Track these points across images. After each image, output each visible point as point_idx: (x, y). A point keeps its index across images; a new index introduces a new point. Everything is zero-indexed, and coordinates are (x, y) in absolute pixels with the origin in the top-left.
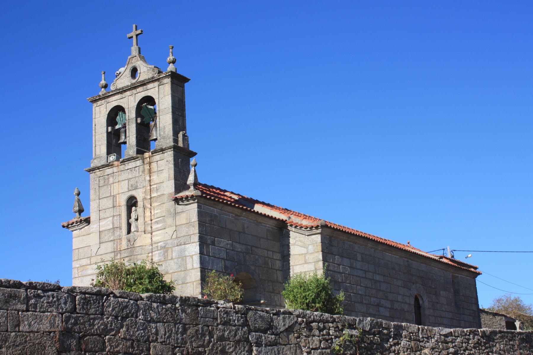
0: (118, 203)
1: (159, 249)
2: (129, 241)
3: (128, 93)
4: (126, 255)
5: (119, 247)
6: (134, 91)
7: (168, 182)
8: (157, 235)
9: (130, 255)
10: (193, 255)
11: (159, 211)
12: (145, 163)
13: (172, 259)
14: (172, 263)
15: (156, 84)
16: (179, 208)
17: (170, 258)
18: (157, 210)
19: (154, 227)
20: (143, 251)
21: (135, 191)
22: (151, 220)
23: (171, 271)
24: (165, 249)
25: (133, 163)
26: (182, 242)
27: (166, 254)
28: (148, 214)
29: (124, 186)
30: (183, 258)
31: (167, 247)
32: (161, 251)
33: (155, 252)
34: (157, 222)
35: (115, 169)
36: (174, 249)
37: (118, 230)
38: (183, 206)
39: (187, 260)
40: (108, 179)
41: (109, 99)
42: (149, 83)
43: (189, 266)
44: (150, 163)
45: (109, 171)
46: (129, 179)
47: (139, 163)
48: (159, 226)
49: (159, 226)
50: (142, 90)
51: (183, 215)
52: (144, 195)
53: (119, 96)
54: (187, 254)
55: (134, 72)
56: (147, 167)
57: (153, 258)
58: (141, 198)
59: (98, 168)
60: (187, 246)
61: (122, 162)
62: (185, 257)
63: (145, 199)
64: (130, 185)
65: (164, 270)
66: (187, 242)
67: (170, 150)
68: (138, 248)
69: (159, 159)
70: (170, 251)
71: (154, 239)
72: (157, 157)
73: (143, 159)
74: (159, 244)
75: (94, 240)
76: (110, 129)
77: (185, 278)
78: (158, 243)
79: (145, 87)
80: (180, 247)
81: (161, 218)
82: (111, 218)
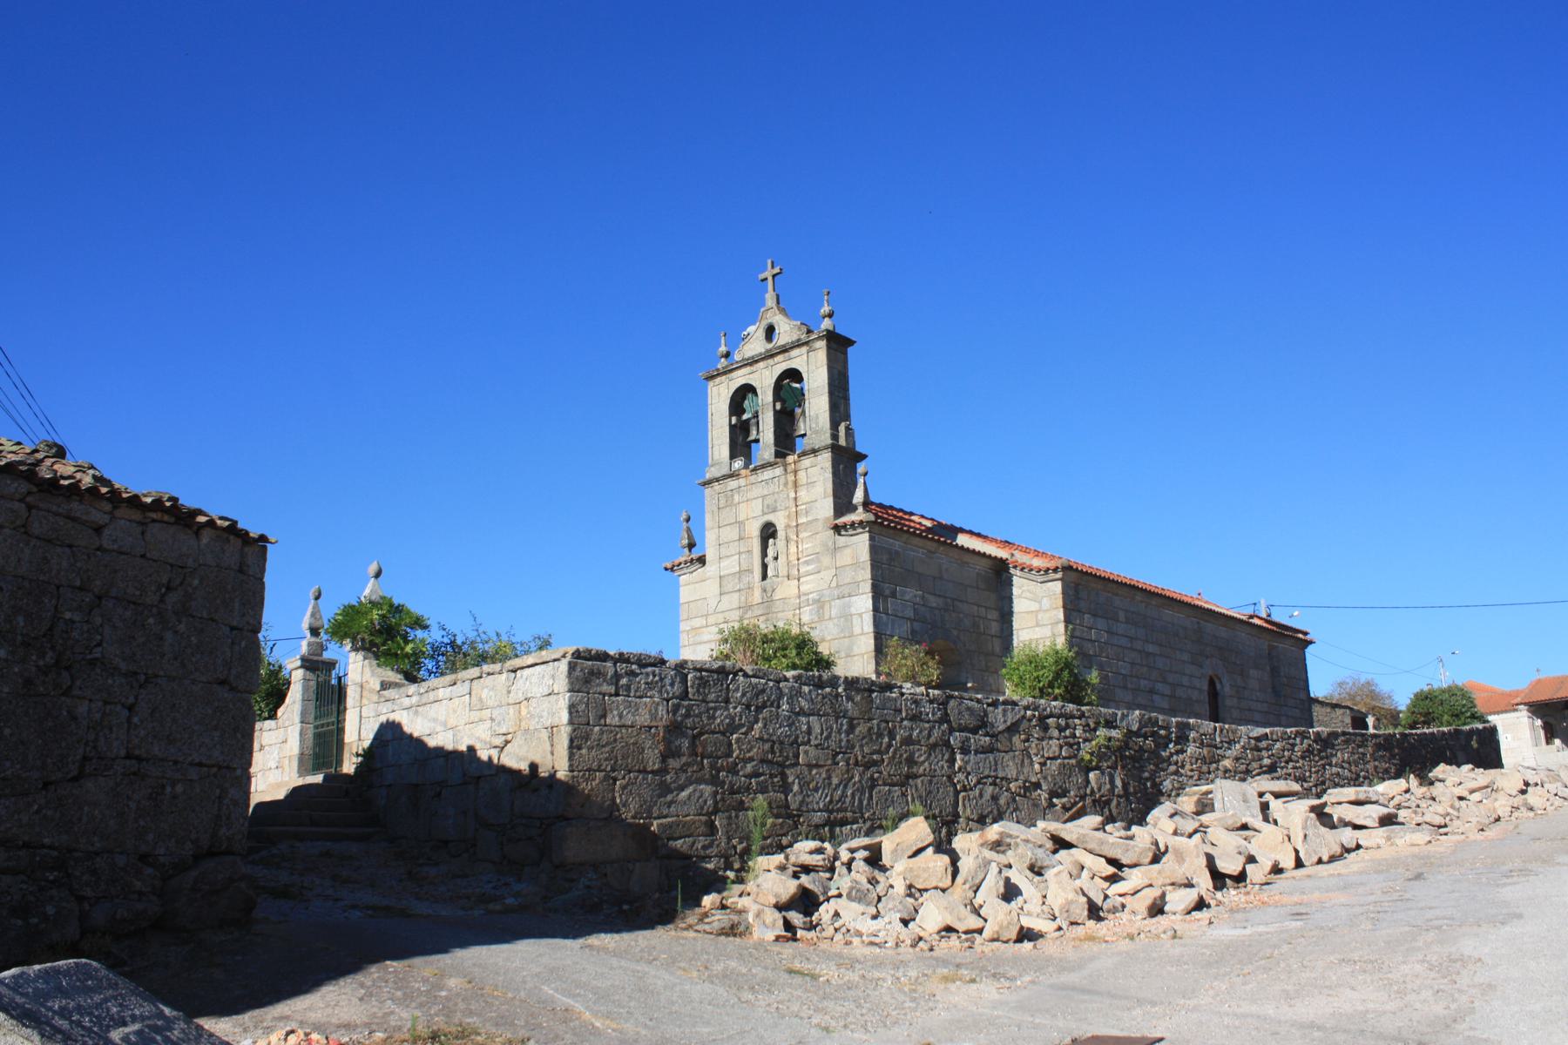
3: (761, 365)
6: (770, 361)
14: (830, 625)
15: (804, 349)
16: (841, 540)
19: (803, 569)
24: (820, 603)
28: (793, 549)
30: (847, 617)
34: (807, 563)
35: (742, 482)
43: (857, 630)
44: (795, 472)
45: (732, 484)
46: (764, 497)
47: (778, 471)
49: (810, 568)
51: (848, 551)
54: (853, 610)
55: (770, 331)
56: (791, 478)
59: (717, 480)
63: (788, 526)
70: (827, 606)
71: (804, 588)
72: (807, 462)
73: (785, 466)
75: (712, 588)
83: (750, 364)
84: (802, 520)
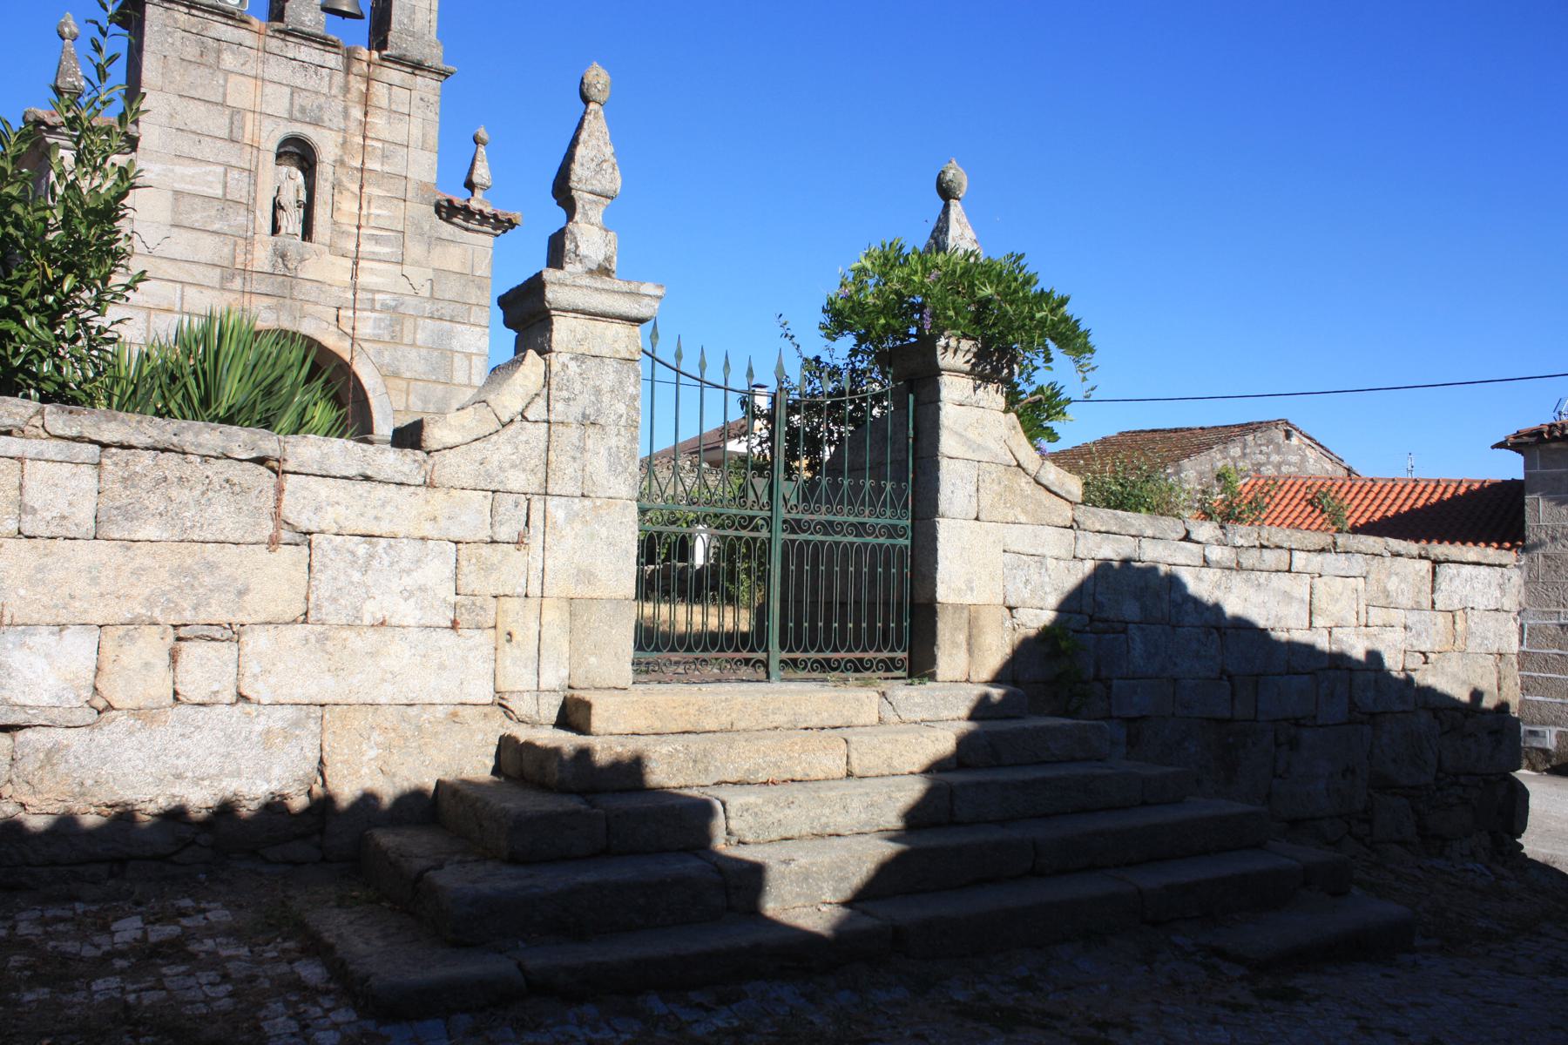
1: (378, 306)
2: (283, 256)
4: (263, 289)
9: (279, 292)
13: (413, 345)
14: (413, 354)
16: (446, 229)
17: (406, 340)
19: (366, 247)
22: (359, 227)
23: (408, 375)
26: (447, 310)
27: (398, 328)
28: (349, 206)
29: (278, 101)
30: (444, 353)
31: (401, 309)
32: (382, 316)
33: (366, 314)
34: (376, 239)
36: (420, 322)
37: (243, 211)
38: (457, 230)
40: (219, 52)
43: (460, 376)
44: (369, 79)
45: (221, 29)
46: (295, 90)
47: (333, 60)
48: (383, 250)
49: (383, 250)
51: (454, 250)
52: (338, 151)
54: (456, 345)
57: (358, 325)
58: (332, 158)
61: (280, 31)
62: (452, 351)
64: (297, 107)
65: (389, 365)
67: (435, 76)
70: (409, 324)
71: (363, 279)
72: (394, 74)
74: (378, 297)
78: (373, 292)
82: (220, 169)
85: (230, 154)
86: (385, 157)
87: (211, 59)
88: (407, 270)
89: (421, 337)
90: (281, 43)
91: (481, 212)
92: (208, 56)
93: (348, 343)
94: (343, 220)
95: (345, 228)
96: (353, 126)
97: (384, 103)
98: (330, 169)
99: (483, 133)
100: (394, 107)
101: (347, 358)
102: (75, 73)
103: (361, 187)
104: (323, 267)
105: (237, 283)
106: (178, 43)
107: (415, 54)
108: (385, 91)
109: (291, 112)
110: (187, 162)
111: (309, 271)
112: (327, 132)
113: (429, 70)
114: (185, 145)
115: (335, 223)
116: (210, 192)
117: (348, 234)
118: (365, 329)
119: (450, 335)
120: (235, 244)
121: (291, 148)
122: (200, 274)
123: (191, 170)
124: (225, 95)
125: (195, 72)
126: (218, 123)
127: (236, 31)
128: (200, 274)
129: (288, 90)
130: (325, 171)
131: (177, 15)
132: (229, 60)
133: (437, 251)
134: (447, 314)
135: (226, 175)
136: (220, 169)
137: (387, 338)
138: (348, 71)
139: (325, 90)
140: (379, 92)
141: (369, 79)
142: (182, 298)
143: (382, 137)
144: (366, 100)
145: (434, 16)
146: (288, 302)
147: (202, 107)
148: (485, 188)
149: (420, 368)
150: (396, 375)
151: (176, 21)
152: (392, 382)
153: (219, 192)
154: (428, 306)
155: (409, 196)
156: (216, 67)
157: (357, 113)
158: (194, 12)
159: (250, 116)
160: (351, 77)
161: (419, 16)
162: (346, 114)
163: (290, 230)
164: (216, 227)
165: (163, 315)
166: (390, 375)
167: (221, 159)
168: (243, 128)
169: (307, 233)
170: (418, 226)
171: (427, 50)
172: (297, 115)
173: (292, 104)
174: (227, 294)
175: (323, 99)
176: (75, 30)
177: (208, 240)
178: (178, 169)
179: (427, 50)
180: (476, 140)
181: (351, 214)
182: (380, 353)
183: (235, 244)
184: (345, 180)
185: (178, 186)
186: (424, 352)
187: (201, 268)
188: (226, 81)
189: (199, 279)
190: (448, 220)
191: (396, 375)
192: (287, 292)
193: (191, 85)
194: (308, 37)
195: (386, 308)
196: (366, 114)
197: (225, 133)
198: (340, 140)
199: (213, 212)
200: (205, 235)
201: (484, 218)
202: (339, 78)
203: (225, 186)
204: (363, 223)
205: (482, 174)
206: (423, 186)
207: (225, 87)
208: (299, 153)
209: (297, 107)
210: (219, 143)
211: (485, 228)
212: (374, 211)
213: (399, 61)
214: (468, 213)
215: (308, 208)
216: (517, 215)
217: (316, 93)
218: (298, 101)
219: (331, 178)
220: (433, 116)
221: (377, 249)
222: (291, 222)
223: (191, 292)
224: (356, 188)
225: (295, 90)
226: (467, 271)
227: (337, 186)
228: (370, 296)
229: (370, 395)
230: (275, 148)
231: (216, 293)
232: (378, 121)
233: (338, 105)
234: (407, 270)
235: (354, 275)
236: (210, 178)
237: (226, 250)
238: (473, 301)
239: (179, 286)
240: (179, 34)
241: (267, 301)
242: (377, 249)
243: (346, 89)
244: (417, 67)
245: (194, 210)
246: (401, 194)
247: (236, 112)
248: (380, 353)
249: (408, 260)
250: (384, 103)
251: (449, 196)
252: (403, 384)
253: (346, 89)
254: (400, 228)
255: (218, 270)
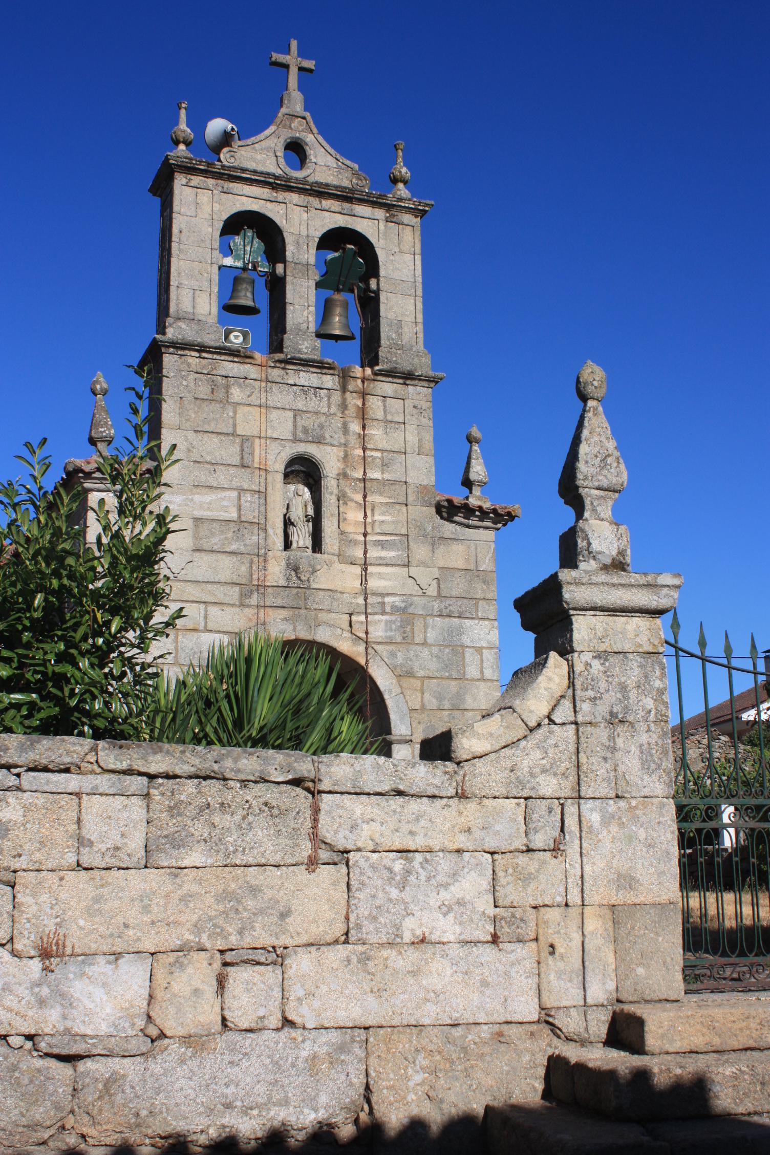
0: (257, 460)
1: (388, 609)
2: (296, 569)
3: (295, 197)
4: (279, 602)
5: (255, 577)
6: (314, 201)
7: (418, 457)
8: (380, 576)
9: (294, 604)
10: (482, 648)
11: (387, 518)
12: (351, 387)
13: (425, 644)
14: (425, 652)
15: (380, 213)
16: (449, 528)
17: (417, 640)
18: (383, 514)
19: (373, 553)
20: (335, 603)
21: (315, 445)
22: (365, 535)
23: (422, 673)
24: (405, 615)
25: (311, 375)
26: (455, 607)
27: (408, 629)
28: (354, 515)
30: (455, 649)
31: (410, 610)
32: (393, 618)
33: (377, 617)
34: (382, 545)
35: (251, 371)
36: (430, 620)
38: (458, 528)
39: (467, 655)
40: (227, 387)
41: (231, 185)
42: (362, 201)
43: (472, 671)
44: (364, 395)
46: (297, 413)
47: (329, 381)
50: (338, 209)
51: (458, 548)
52: (340, 465)
53: (265, 192)
54: (466, 640)
57: (370, 629)
59: (202, 349)
60: (468, 623)
61: (280, 361)
62: (463, 646)
63: (344, 475)
64: (300, 429)
65: (402, 665)
66: (468, 615)
68: (322, 593)
69: (390, 394)
70: (419, 623)
71: (373, 584)
72: (387, 387)
74: (387, 600)
76: (373, 283)
77: (460, 695)
78: (383, 595)
79: (347, 205)
80: (447, 619)
81: (396, 538)
82: (234, 494)
83: (274, 187)
84: (374, 474)
85: (243, 479)
86: (384, 466)
87: (220, 394)
88: (413, 571)
89: (431, 635)
90: (281, 372)
91: (480, 508)
92: (219, 393)
93: (361, 648)
94: (349, 529)
95: (351, 536)
96: (353, 440)
97: (380, 414)
98: (334, 483)
99: (475, 432)
100: (389, 418)
101: (362, 662)
102: (106, 423)
103: (365, 497)
104: (336, 577)
105: (254, 600)
106: (192, 385)
107: (405, 365)
108: (380, 403)
109: (294, 434)
110: (204, 490)
111: (322, 581)
112: (329, 448)
113: (419, 378)
114: (203, 476)
115: (342, 533)
116: (225, 516)
117: (355, 542)
118: (378, 632)
119: (460, 631)
120: (252, 562)
121: (296, 467)
122: (220, 593)
123: (209, 497)
124: (235, 426)
125: (207, 408)
126: (230, 452)
127: (241, 367)
128: (220, 593)
129: (290, 414)
130: (330, 485)
131: (190, 360)
132: (236, 394)
133: (441, 550)
134: (456, 609)
135: (239, 499)
136: (234, 494)
137: (399, 639)
138: (344, 389)
139: (325, 410)
140: (375, 405)
141: (364, 395)
142: (206, 617)
143: (380, 446)
144: (363, 415)
145: (420, 328)
146: (303, 612)
147: (215, 439)
148: (482, 484)
149: (433, 666)
150: (410, 674)
151: (189, 365)
152: (406, 682)
153: (234, 515)
154: (436, 605)
155: (411, 499)
156: (226, 401)
157: (355, 427)
158: (204, 355)
159: (257, 441)
160: (348, 395)
161: (406, 329)
162: (345, 429)
163: (301, 544)
164: (233, 547)
165: (190, 635)
166: (404, 674)
167: (235, 484)
168: (252, 454)
169: (317, 545)
170: (420, 527)
171: (416, 360)
172: (301, 435)
173: (295, 426)
174: (247, 610)
175: (323, 418)
176: (105, 386)
177: (227, 562)
178: (197, 498)
179: (416, 360)
180: (470, 440)
181: (356, 523)
182: (393, 654)
183: (252, 562)
184: (348, 490)
185: (198, 513)
186: (435, 650)
187: (222, 588)
188: (235, 412)
189: (220, 597)
190: (449, 519)
191: (410, 674)
192: (301, 603)
193: (206, 421)
194: (306, 363)
195: (396, 610)
196: (364, 427)
197: (236, 460)
198: (342, 454)
199: (230, 534)
200: (224, 556)
201: (484, 514)
202: (336, 397)
203: (239, 509)
204: (369, 530)
205: (478, 470)
206: (423, 490)
207: (234, 418)
208: (305, 471)
209: (300, 429)
210: (232, 471)
211: (486, 524)
212: (377, 518)
213: (391, 374)
214: (468, 511)
215: (316, 521)
216: (516, 508)
217: (317, 413)
218: (301, 423)
219: (335, 491)
220: (427, 422)
221: (384, 554)
222: (302, 537)
223: (213, 610)
224: (359, 498)
225: (297, 413)
226: (472, 567)
227: (342, 498)
228: (379, 600)
229: (386, 696)
230: (282, 468)
231: (237, 609)
232: (376, 432)
233: (337, 423)
234: (413, 571)
235: (364, 579)
236: (225, 503)
237: (244, 569)
238: (480, 596)
239: (202, 606)
240: (193, 376)
241: (284, 613)
242: (384, 554)
243: (344, 406)
244: (408, 377)
245: (213, 534)
246: (402, 499)
247: (246, 440)
248: (393, 654)
249: (414, 562)
250: (380, 414)
251: (447, 497)
252: (418, 683)
253: (344, 406)
254: (404, 531)
255: (237, 588)
